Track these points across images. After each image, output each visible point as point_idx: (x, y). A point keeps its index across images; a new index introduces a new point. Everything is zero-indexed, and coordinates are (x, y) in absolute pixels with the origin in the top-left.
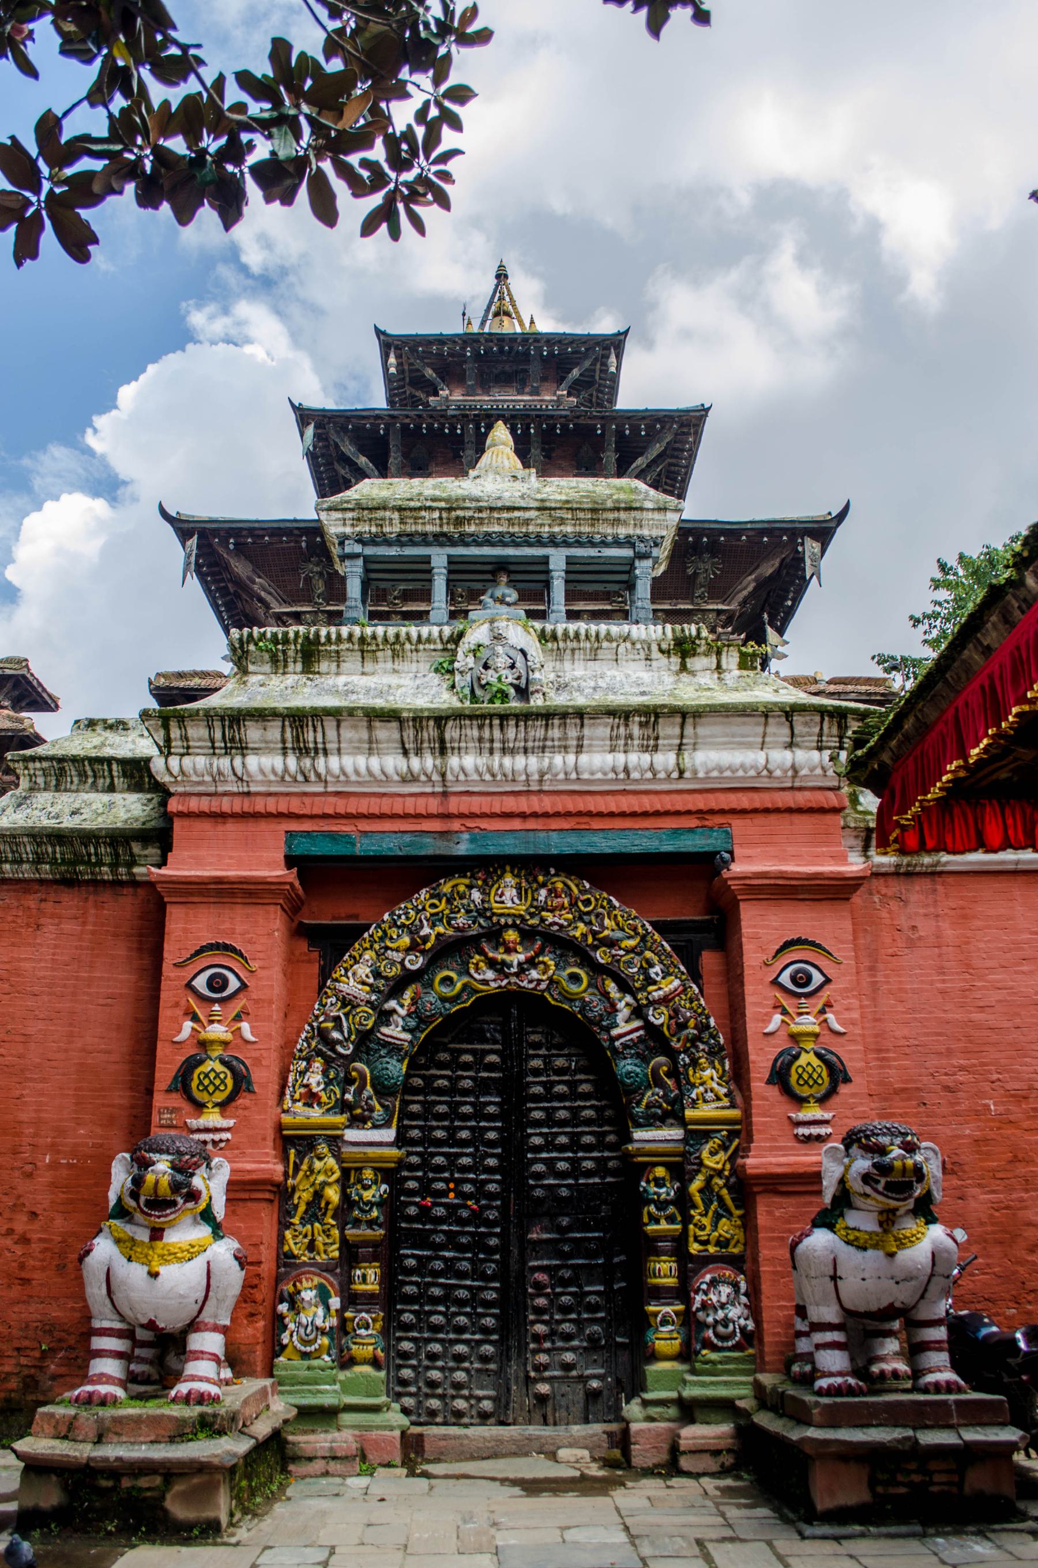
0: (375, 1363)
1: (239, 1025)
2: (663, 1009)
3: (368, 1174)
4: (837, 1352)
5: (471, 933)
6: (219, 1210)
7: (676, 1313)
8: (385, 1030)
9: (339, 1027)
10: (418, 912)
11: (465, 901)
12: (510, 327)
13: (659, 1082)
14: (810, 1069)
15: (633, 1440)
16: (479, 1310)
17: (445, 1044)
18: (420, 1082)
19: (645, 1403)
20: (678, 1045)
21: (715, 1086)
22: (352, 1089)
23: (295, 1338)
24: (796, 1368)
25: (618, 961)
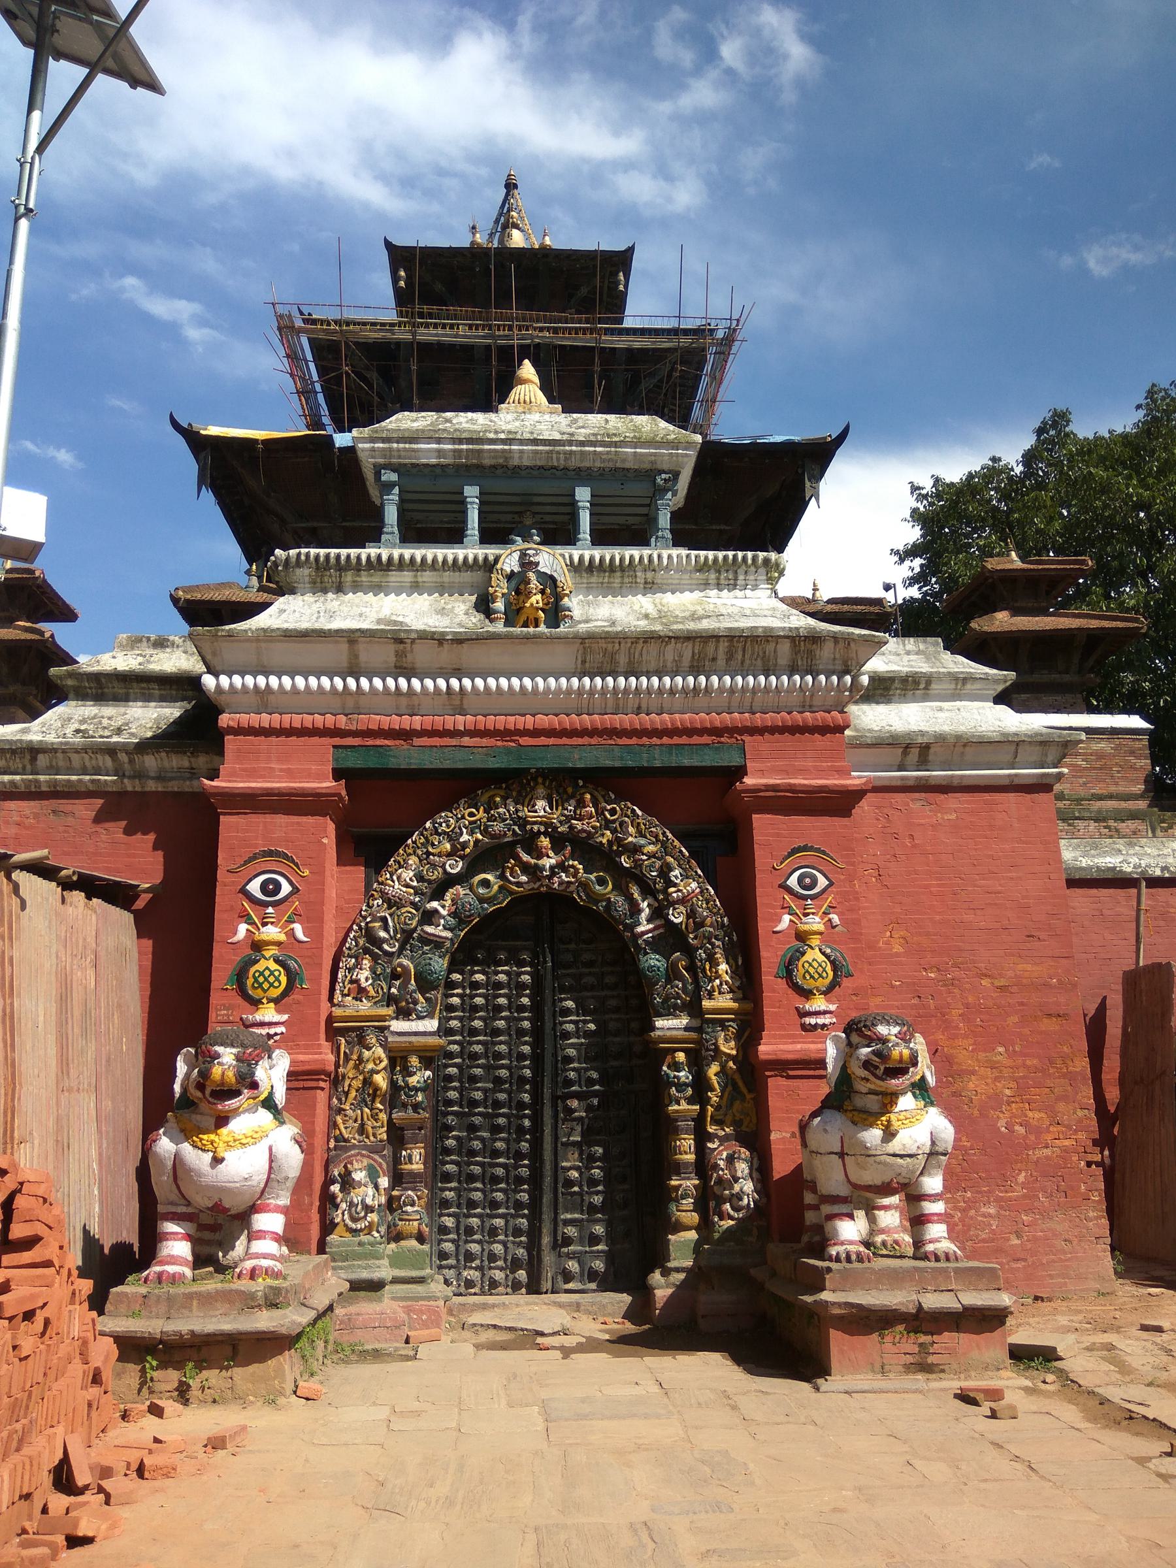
0: (421, 1238)
1: (292, 926)
2: (682, 909)
3: (414, 1061)
6: (280, 1097)
7: (695, 1186)
8: (430, 929)
9: (386, 929)
10: (458, 820)
14: (815, 964)
18: (459, 976)
22: (397, 983)
23: (346, 1216)
25: (641, 865)
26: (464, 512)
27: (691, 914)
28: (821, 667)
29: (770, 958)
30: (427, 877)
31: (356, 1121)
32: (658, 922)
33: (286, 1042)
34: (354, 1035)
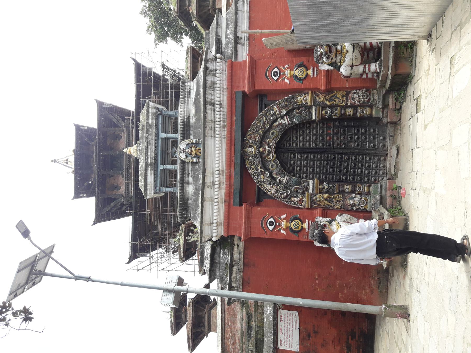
0: (369, 186)
3: (321, 187)
4: (371, 66)
5: (260, 160)
6: (328, 219)
7: (360, 109)
8: (284, 182)
9: (283, 193)
10: (254, 173)
11: (252, 161)
12: (72, 159)
13: (300, 113)
15: (392, 121)
16: (357, 160)
17: (288, 168)
18: (298, 174)
19: (383, 117)
20: (291, 107)
21: (302, 97)
24: (375, 78)
25: (269, 122)
26: (167, 169)
27: (283, 108)
28: (214, 68)
29: (297, 84)
30: (270, 182)
31: (336, 203)
32: (285, 118)
33: (313, 221)
34: (312, 203)
